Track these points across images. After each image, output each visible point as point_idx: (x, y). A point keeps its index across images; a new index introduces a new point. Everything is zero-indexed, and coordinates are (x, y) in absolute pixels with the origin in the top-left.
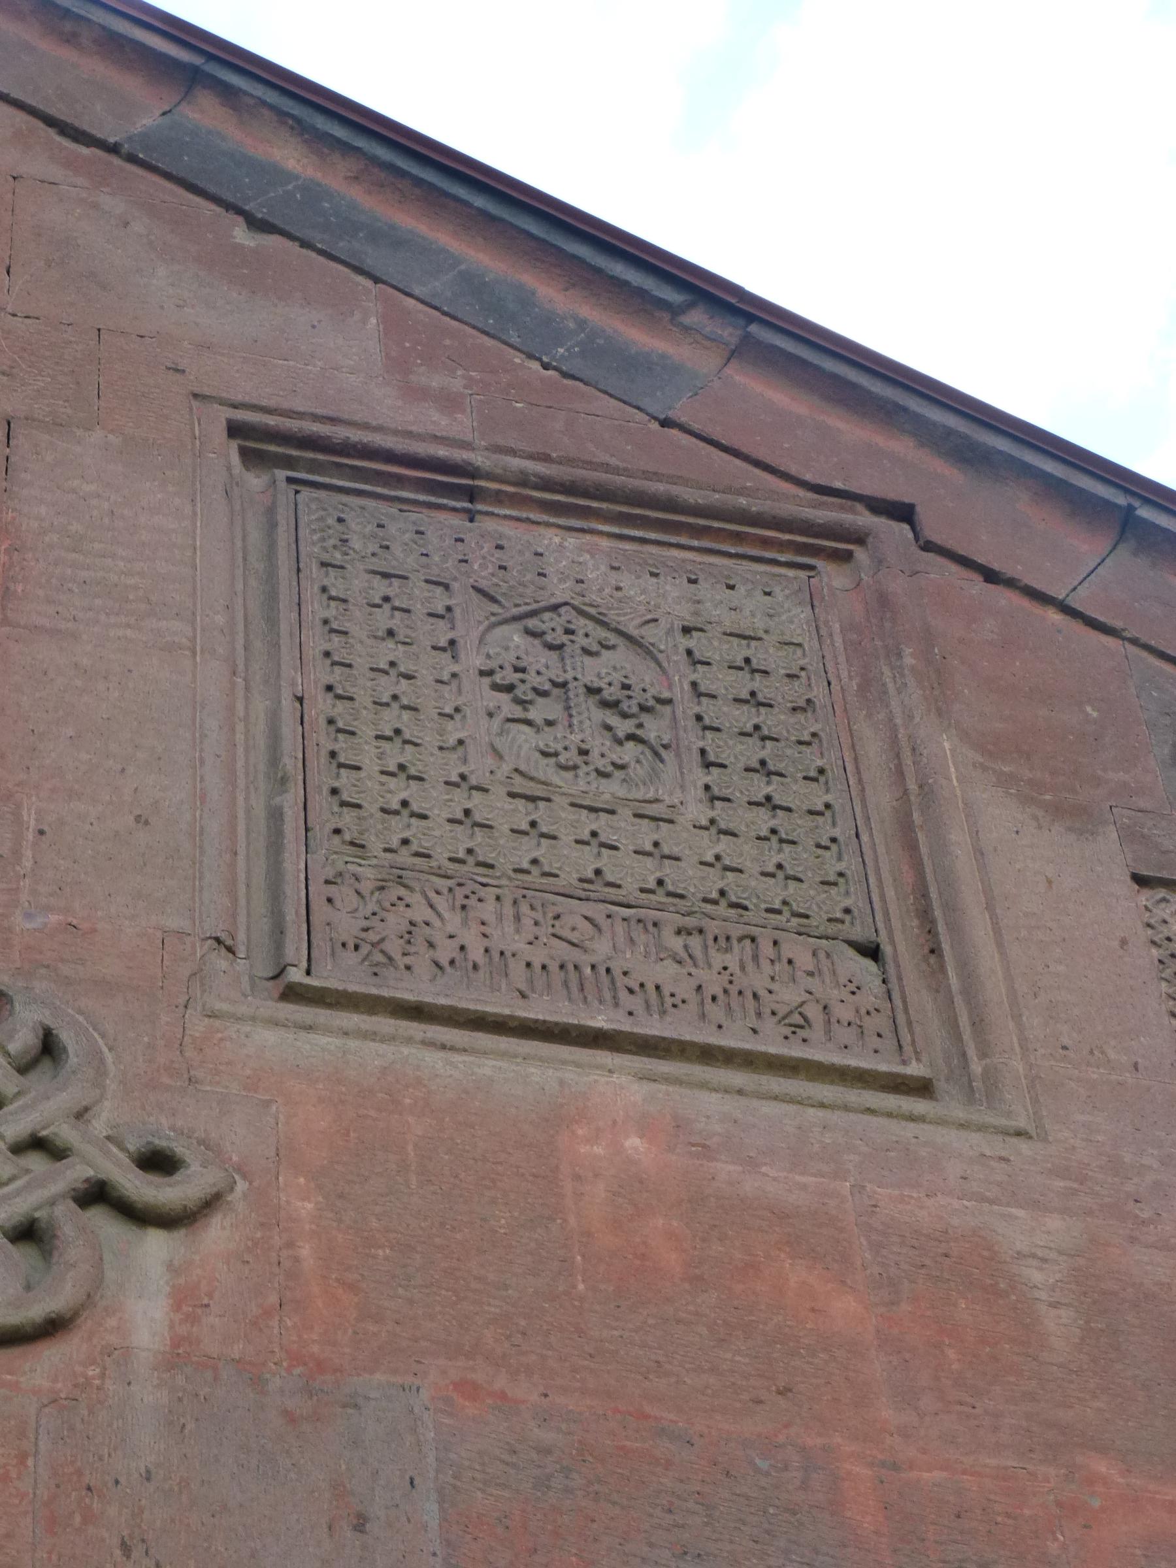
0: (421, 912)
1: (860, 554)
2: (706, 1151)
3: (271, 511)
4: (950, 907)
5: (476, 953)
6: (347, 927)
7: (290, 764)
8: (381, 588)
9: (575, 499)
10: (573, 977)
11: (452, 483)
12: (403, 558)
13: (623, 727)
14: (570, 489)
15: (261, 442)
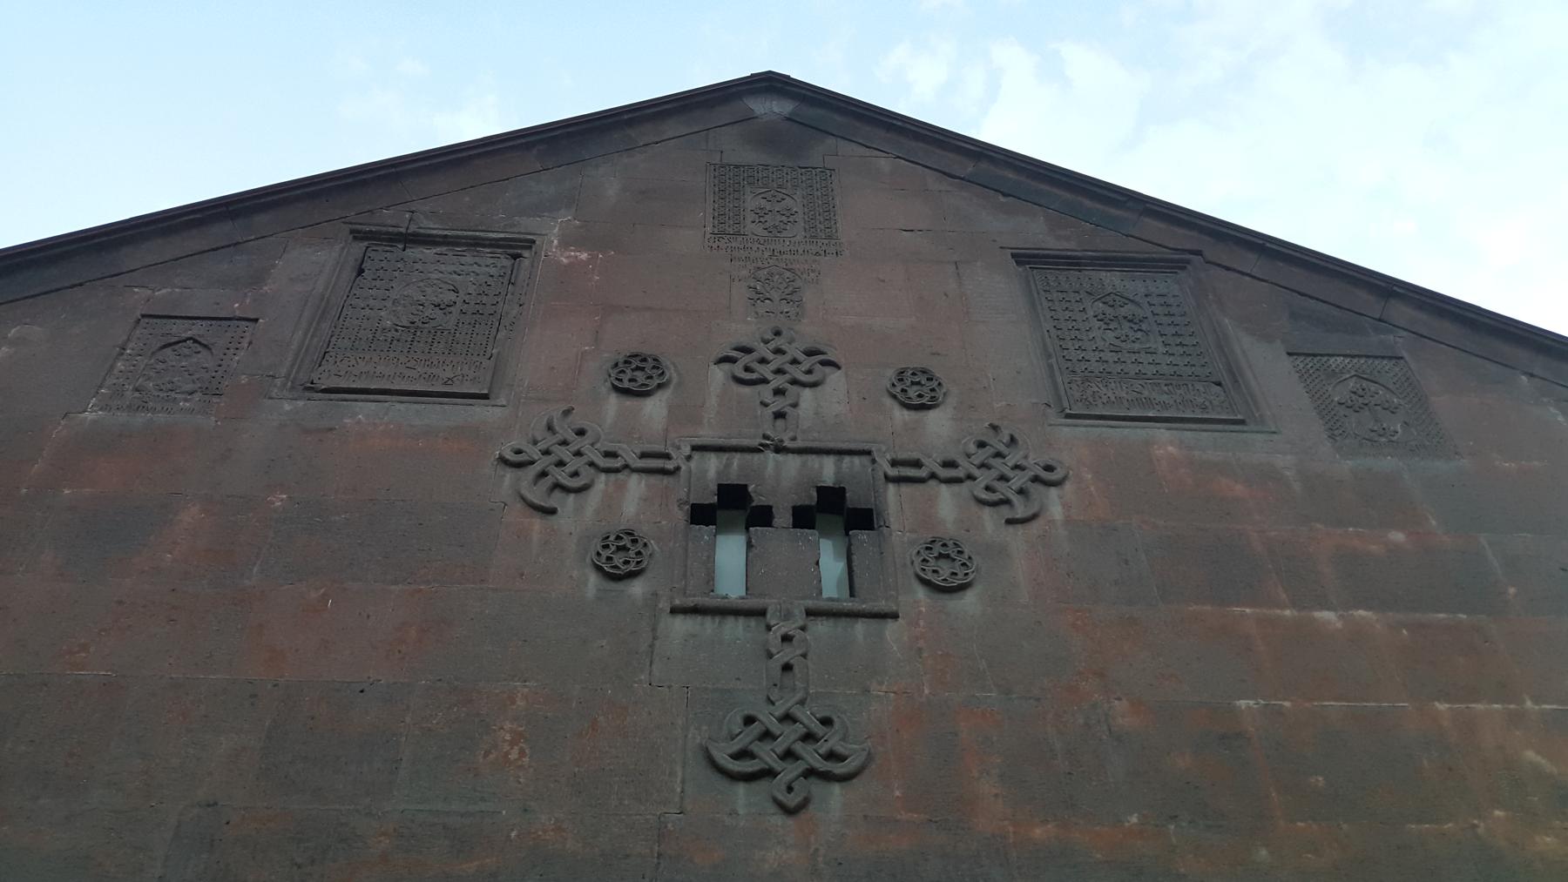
6: (1077, 395)
8: (1061, 296)
9: (1108, 262)
14: (1106, 259)
15: (1021, 258)
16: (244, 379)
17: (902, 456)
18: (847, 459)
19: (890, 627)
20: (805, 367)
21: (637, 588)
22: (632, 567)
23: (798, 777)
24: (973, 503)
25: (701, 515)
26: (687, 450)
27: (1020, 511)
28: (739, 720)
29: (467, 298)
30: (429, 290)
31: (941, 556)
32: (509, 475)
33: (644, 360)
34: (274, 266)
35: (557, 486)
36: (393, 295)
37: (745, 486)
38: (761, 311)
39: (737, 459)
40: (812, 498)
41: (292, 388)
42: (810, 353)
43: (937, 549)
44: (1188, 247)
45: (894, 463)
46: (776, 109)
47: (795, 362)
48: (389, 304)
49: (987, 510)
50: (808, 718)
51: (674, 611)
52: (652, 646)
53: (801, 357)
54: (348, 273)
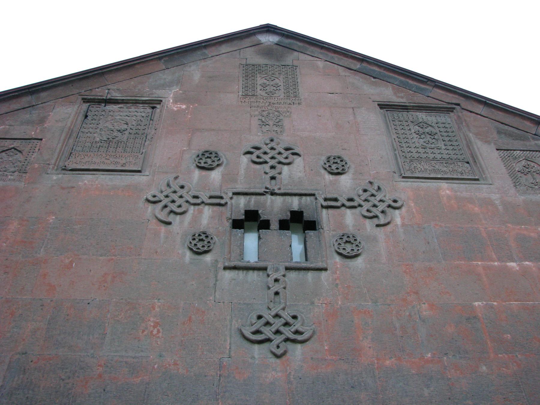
0: (415, 165)
1: (454, 111)
2: (456, 192)
3: (385, 114)
4: (476, 156)
5: (423, 169)
6: (407, 168)
7: (396, 148)
8: (400, 123)
10: (435, 171)
11: (404, 108)
12: (402, 119)
13: (433, 137)
15: (382, 106)
16: (36, 166)
17: (329, 196)
18: (304, 198)
19: (324, 274)
20: (284, 156)
21: (208, 258)
22: (206, 248)
23: (281, 342)
24: (361, 217)
25: (237, 224)
26: (230, 195)
27: (382, 221)
28: (255, 317)
29: (132, 127)
30: (115, 124)
31: (347, 242)
32: (150, 207)
33: (211, 153)
34: (49, 115)
35: (172, 212)
36: (100, 126)
37: (257, 211)
38: (265, 130)
39: (253, 198)
40: (288, 216)
41: (56, 170)
42: (287, 149)
43: (345, 239)
44: (454, 102)
45: (326, 200)
46: (271, 40)
47: (280, 153)
48: (98, 130)
49: (368, 220)
50: (286, 316)
51: (225, 268)
52: (215, 284)
53: (283, 151)
54: (81, 117)
